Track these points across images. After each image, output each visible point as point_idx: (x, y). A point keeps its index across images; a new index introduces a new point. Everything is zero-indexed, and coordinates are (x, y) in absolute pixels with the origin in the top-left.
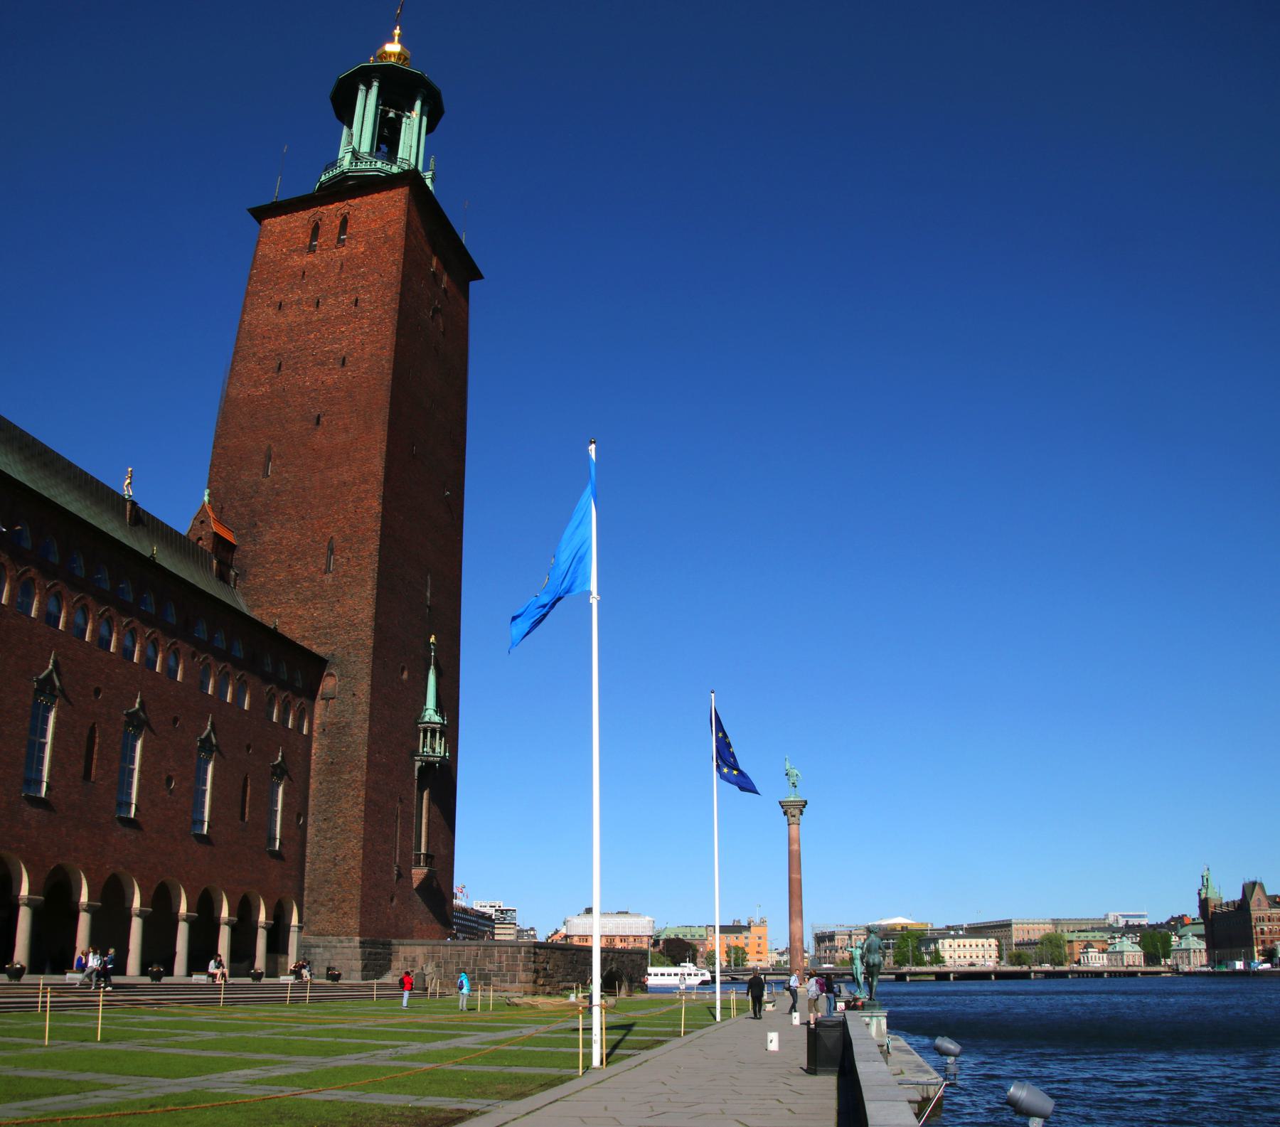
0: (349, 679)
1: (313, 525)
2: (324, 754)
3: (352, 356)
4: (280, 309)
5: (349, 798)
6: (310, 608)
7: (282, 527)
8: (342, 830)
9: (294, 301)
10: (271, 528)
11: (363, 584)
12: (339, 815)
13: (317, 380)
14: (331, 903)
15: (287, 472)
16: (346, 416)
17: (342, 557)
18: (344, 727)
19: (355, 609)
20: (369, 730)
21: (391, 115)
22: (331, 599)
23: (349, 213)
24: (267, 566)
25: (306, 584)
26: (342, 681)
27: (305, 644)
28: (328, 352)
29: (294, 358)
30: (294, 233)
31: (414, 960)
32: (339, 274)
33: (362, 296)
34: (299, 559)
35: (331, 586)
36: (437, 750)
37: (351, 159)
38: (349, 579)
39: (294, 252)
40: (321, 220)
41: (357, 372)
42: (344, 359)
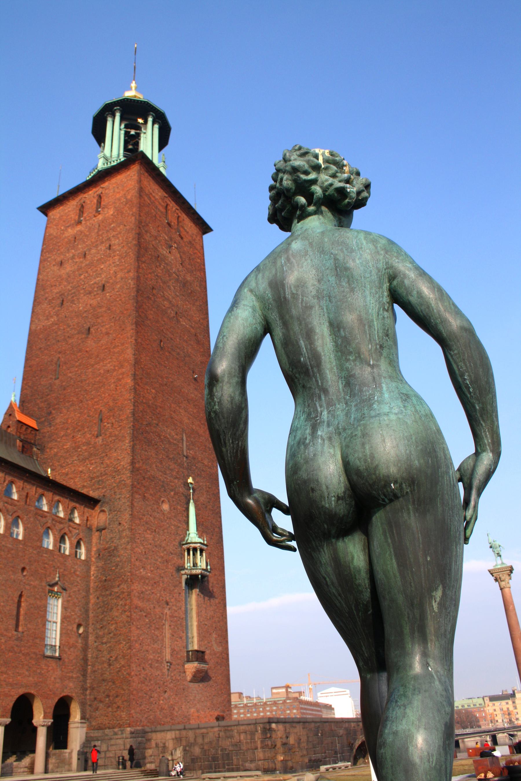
0: (116, 512)
2: (99, 574)
5: (119, 607)
6: (87, 464)
7: (68, 411)
8: (115, 635)
10: (61, 413)
12: (112, 622)
13: (87, 304)
14: (107, 699)
15: (70, 372)
17: (108, 423)
18: (113, 550)
19: (118, 459)
21: (133, 132)
24: (59, 440)
25: (84, 448)
27: (84, 491)
28: (93, 284)
29: (71, 294)
30: (68, 216)
31: (164, 747)
32: (98, 233)
34: (79, 431)
35: (101, 445)
36: (199, 564)
38: (113, 438)
39: (68, 227)
40: (84, 202)
42: (104, 286)
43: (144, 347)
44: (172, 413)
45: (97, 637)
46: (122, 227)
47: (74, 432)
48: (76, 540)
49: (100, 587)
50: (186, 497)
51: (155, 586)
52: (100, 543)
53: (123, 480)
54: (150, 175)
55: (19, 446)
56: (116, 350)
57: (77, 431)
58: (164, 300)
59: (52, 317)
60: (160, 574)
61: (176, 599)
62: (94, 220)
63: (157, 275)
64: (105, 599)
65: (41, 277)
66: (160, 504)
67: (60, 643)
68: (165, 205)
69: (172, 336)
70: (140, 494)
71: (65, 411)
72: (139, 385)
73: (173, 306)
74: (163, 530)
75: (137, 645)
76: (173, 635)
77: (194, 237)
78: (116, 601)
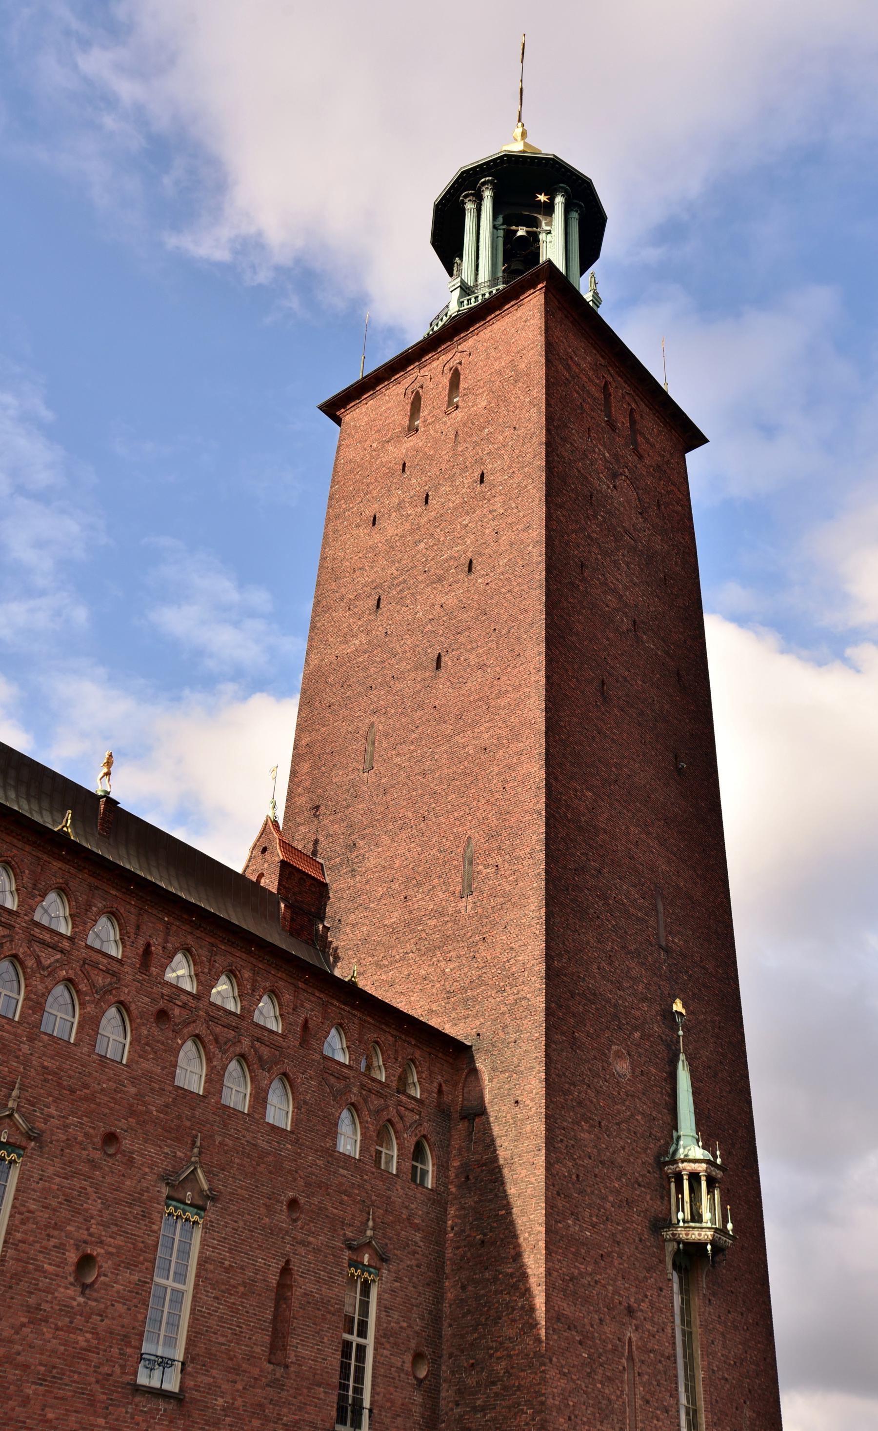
0: (507, 1074)
1: (439, 825)
3: (481, 554)
4: (374, 524)
5: (516, 1314)
8: (505, 1388)
9: (393, 507)
11: (524, 902)
12: (499, 1354)
15: (398, 754)
16: (479, 644)
17: (486, 867)
19: (512, 949)
20: (547, 1169)
21: (521, 232)
22: (472, 940)
23: (460, 363)
26: (495, 1081)
27: (433, 1022)
28: (446, 561)
33: (490, 466)
34: (419, 884)
37: (461, 296)
41: (492, 575)
42: (471, 562)
43: (565, 695)
44: (630, 846)
45: (459, 1392)
46: (508, 432)
47: (407, 888)
48: (414, 1140)
49: (469, 1261)
50: (668, 1047)
51: (603, 1263)
52: (468, 1150)
53: (524, 998)
54: (566, 317)
55: (284, 918)
56: (503, 702)
57: (415, 886)
58: (605, 592)
59: (355, 636)
60: (613, 1234)
61: (651, 1303)
62: (445, 423)
63: (589, 537)
64: (482, 1292)
65: (329, 552)
66: (610, 1060)
67: (372, 1403)
68: (602, 385)
69: (627, 673)
70: (563, 1034)
71: (385, 840)
72: (556, 779)
73: (626, 605)
74: (618, 1124)
75: (562, 1420)
76: (648, 1402)
77: (667, 455)
78: (507, 1297)
